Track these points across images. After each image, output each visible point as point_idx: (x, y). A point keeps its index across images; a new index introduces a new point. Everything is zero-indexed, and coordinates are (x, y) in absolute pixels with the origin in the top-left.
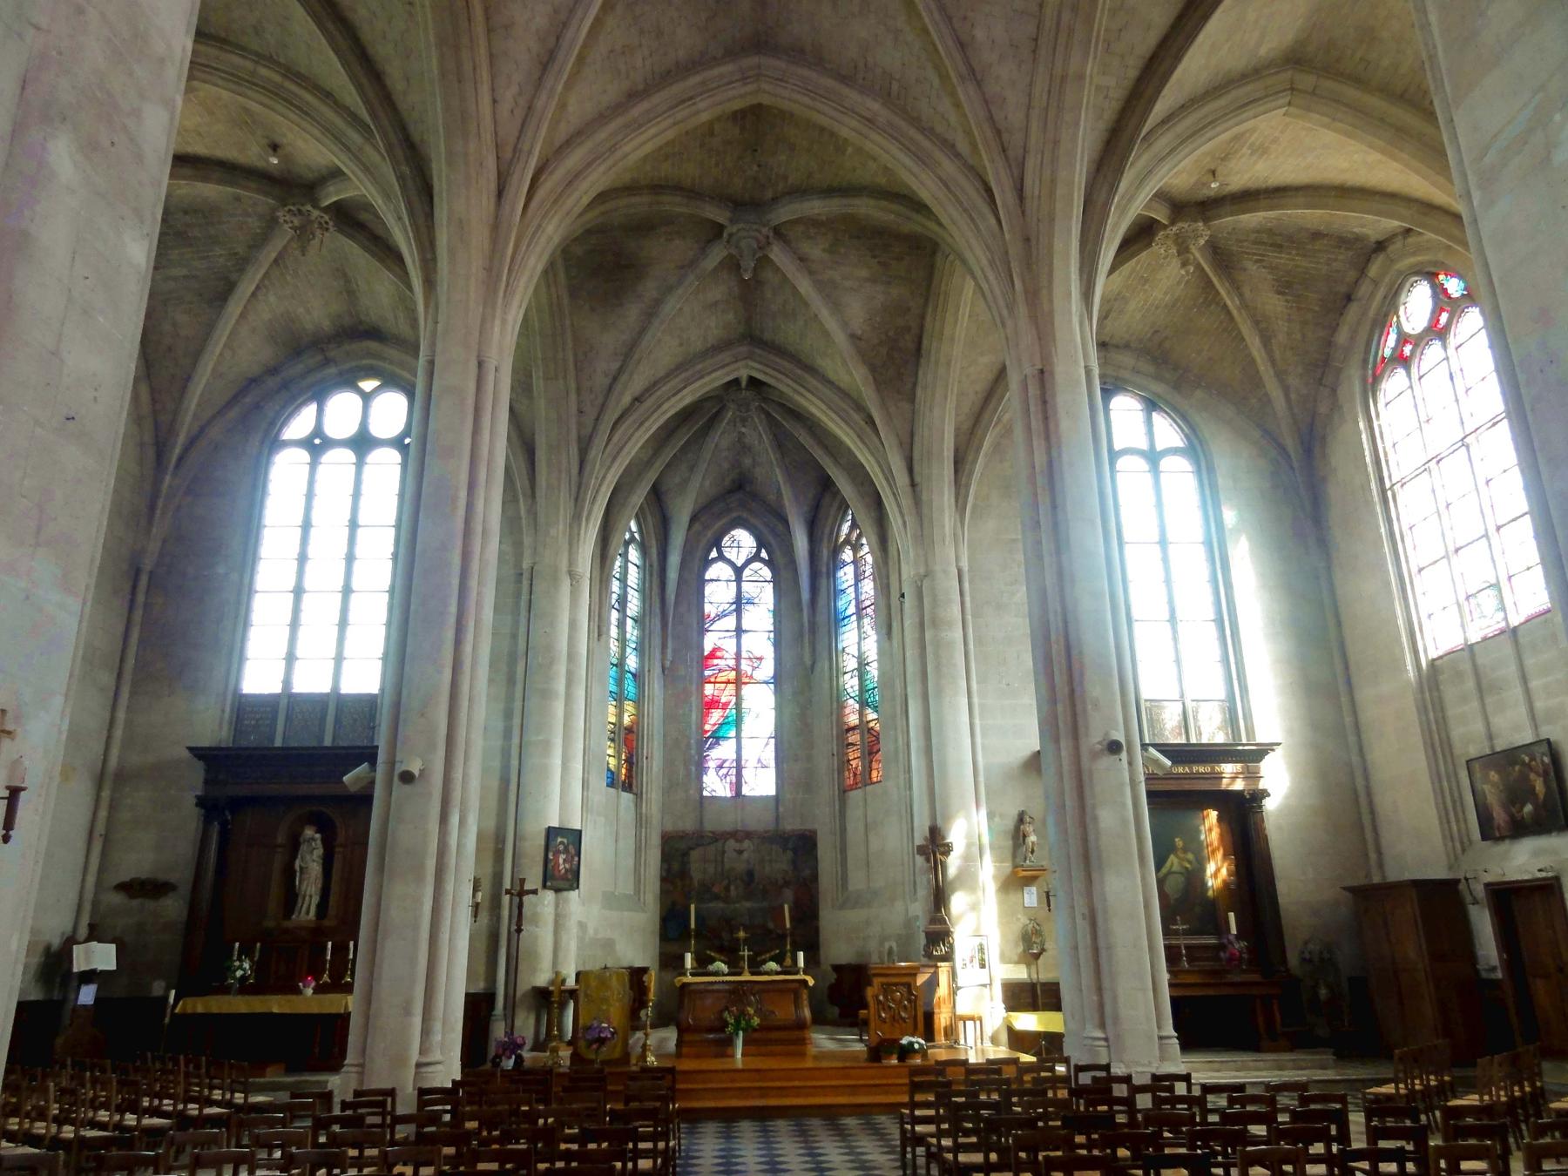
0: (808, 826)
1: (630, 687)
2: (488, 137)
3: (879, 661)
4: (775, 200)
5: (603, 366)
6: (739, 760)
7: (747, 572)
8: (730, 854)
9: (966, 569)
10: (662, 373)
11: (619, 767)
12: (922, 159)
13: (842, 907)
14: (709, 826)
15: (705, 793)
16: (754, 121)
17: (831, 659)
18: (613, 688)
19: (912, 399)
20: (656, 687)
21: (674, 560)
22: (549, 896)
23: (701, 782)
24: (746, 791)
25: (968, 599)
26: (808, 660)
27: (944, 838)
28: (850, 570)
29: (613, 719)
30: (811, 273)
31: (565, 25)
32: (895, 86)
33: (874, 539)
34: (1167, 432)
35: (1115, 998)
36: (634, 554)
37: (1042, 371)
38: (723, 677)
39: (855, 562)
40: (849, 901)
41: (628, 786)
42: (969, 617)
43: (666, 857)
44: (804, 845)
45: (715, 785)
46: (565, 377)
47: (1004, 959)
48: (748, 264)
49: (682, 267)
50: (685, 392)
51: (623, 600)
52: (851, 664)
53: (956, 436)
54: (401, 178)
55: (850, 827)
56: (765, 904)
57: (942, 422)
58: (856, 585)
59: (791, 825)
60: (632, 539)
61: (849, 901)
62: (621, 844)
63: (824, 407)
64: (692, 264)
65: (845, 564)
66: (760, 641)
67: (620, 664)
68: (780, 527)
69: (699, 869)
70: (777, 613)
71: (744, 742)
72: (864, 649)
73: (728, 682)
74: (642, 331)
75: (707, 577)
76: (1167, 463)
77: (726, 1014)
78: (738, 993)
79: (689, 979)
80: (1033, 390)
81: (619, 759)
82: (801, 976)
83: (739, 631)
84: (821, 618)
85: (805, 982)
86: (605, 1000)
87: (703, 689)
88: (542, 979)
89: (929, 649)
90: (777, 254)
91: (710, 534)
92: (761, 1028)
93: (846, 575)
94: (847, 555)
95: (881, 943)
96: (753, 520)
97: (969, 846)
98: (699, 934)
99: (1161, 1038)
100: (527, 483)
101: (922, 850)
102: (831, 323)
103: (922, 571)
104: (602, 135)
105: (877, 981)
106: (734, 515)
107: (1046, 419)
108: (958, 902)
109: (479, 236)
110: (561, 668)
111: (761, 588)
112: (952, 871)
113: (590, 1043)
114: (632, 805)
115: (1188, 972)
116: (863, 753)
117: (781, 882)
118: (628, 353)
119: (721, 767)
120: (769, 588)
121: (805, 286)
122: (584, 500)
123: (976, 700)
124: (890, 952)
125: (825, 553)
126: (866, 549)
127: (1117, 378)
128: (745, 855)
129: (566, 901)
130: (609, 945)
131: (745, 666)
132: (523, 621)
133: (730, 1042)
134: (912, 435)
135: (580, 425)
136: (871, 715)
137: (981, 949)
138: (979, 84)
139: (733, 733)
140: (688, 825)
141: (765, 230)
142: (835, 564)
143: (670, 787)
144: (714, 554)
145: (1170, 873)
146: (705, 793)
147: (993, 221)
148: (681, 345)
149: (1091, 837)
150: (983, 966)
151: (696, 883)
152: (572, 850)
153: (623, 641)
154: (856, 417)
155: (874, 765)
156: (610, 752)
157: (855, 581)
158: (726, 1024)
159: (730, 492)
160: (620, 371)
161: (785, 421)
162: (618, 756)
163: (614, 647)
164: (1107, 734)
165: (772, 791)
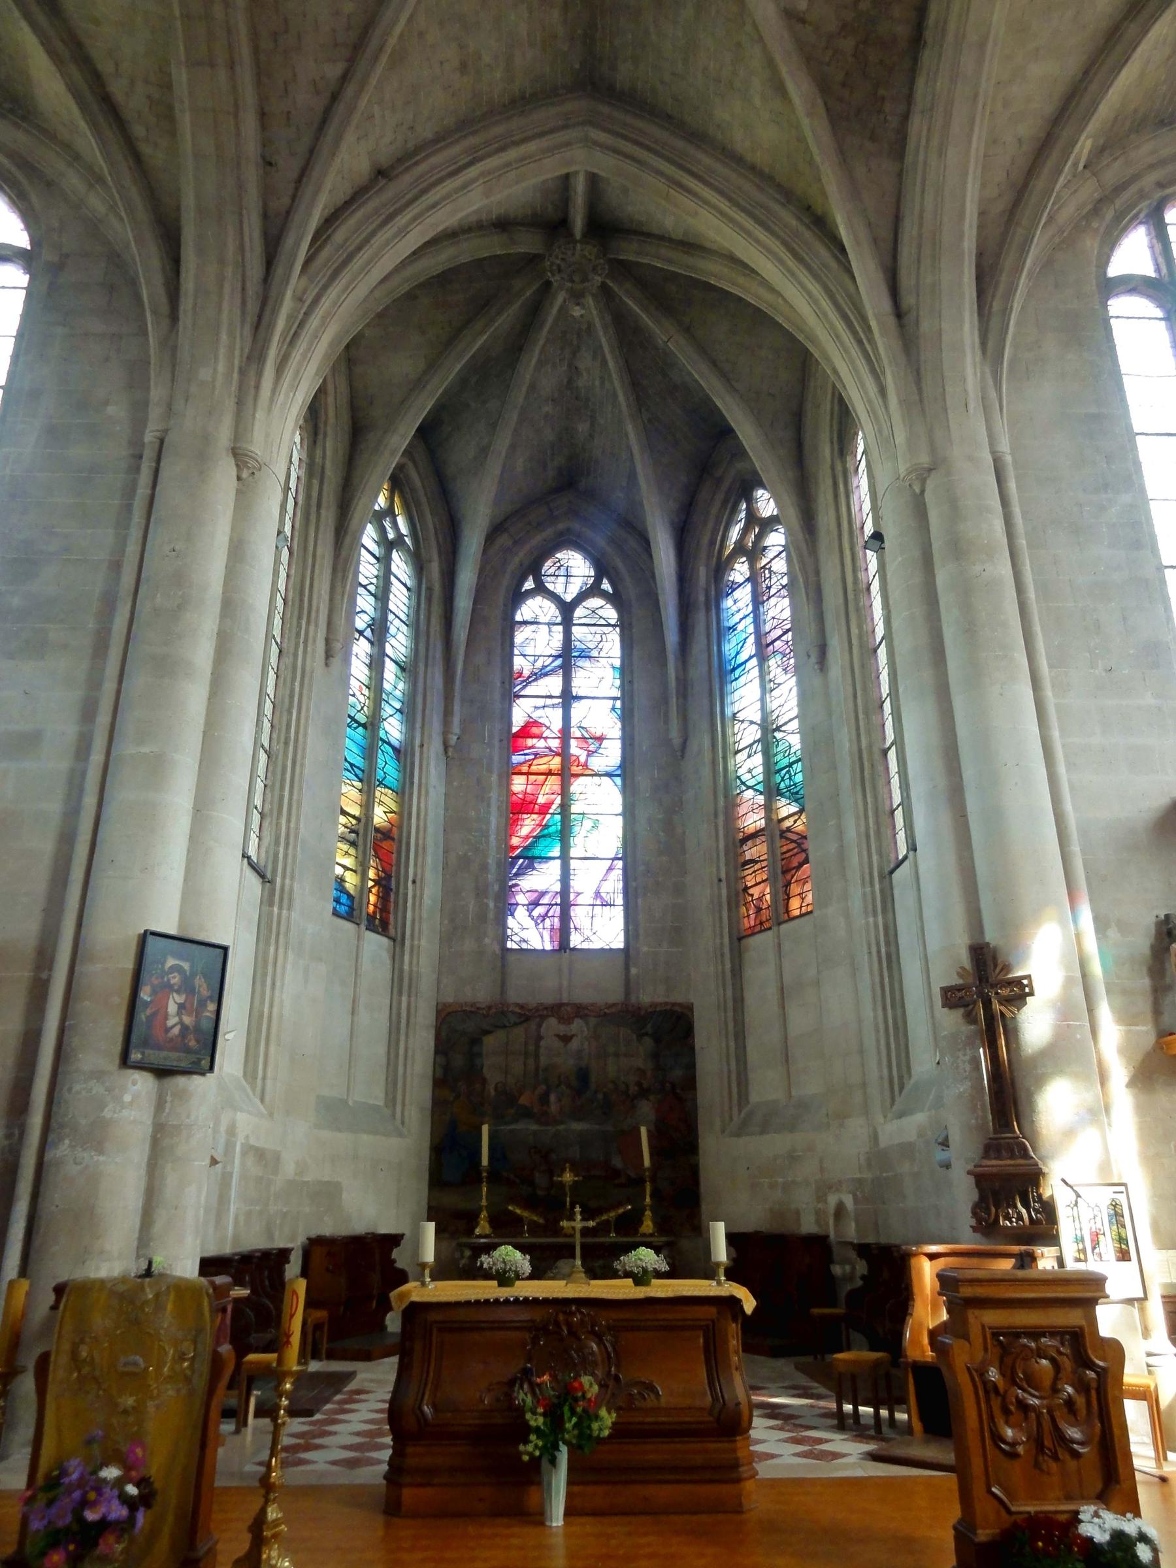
0: (678, 997)
1: (387, 766)
5: (314, 68)
6: (565, 891)
7: (579, 612)
8: (549, 1042)
9: (1008, 459)
10: (427, 132)
11: (363, 890)
14: (515, 996)
18: (358, 761)
19: (898, 148)
20: (432, 772)
21: (467, 578)
22: (141, 1084)
23: (505, 927)
24: (575, 941)
25: (1017, 510)
26: (675, 735)
27: (1007, 968)
28: (744, 595)
29: (355, 811)
36: (400, 566)
38: (540, 765)
39: (753, 579)
40: (750, 1120)
41: (381, 923)
42: (1022, 542)
43: (443, 1047)
44: (672, 1029)
45: (527, 931)
46: (231, 65)
50: (472, 172)
51: (379, 630)
52: (748, 734)
53: (981, 227)
55: (750, 997)
57: (960, 176)
58: (756, 612)
59: (649, 996)
61: (750, 1120)
62: (364, 1017)
63: (724, 205)
65: (734, 587)
66: (599, 714)
67: (372, 725)
68: (633, 543)
69: (498, 1063)
70: (626, 671)
72: (772, 705)
73: (550, 773)
75: (518, 618)
77: (523, 1397)
78: (555, 1330)
81: (364, 877)
83: (568, 698)
84: (697, 672)
86: (136, 1379)
87: (509, 783)
94: (740, 571)
95: (821, 1198)
96: (588, 533)
98: (495, 1176)
100: (161, 292)
103: (924, 459)
106: (561, 526)
108: (1056, 1105)
111: (602, 634)
113: (55, 1538)
114: (386, 957)
117: (633, 1089)
120: (614, 636)
122: (271, 326)
123: (1048, 693)
124: (840, 1211)
125: (702, 574)
128: (574, 1044)
129: (182, 1096)
130: (327, 1193)
131: (574, 749)
132: (135, 533)
133: (532, 1475)
134: (897, 221)
135: (267, 192)
136: (785, 808)
139: (556, 851)
140: (481, 993)
142: (720, 588)
143: (455, 927)
144: (529, 584)
146: (509, 945)
148: (463, 67)
150: (1124, 1256)
152: (202, 986)
155: (795, 889)
156: (349, 862)
157: (757, 605)
160: (345, 78)
162: (361, 870)
165: (617, 941)
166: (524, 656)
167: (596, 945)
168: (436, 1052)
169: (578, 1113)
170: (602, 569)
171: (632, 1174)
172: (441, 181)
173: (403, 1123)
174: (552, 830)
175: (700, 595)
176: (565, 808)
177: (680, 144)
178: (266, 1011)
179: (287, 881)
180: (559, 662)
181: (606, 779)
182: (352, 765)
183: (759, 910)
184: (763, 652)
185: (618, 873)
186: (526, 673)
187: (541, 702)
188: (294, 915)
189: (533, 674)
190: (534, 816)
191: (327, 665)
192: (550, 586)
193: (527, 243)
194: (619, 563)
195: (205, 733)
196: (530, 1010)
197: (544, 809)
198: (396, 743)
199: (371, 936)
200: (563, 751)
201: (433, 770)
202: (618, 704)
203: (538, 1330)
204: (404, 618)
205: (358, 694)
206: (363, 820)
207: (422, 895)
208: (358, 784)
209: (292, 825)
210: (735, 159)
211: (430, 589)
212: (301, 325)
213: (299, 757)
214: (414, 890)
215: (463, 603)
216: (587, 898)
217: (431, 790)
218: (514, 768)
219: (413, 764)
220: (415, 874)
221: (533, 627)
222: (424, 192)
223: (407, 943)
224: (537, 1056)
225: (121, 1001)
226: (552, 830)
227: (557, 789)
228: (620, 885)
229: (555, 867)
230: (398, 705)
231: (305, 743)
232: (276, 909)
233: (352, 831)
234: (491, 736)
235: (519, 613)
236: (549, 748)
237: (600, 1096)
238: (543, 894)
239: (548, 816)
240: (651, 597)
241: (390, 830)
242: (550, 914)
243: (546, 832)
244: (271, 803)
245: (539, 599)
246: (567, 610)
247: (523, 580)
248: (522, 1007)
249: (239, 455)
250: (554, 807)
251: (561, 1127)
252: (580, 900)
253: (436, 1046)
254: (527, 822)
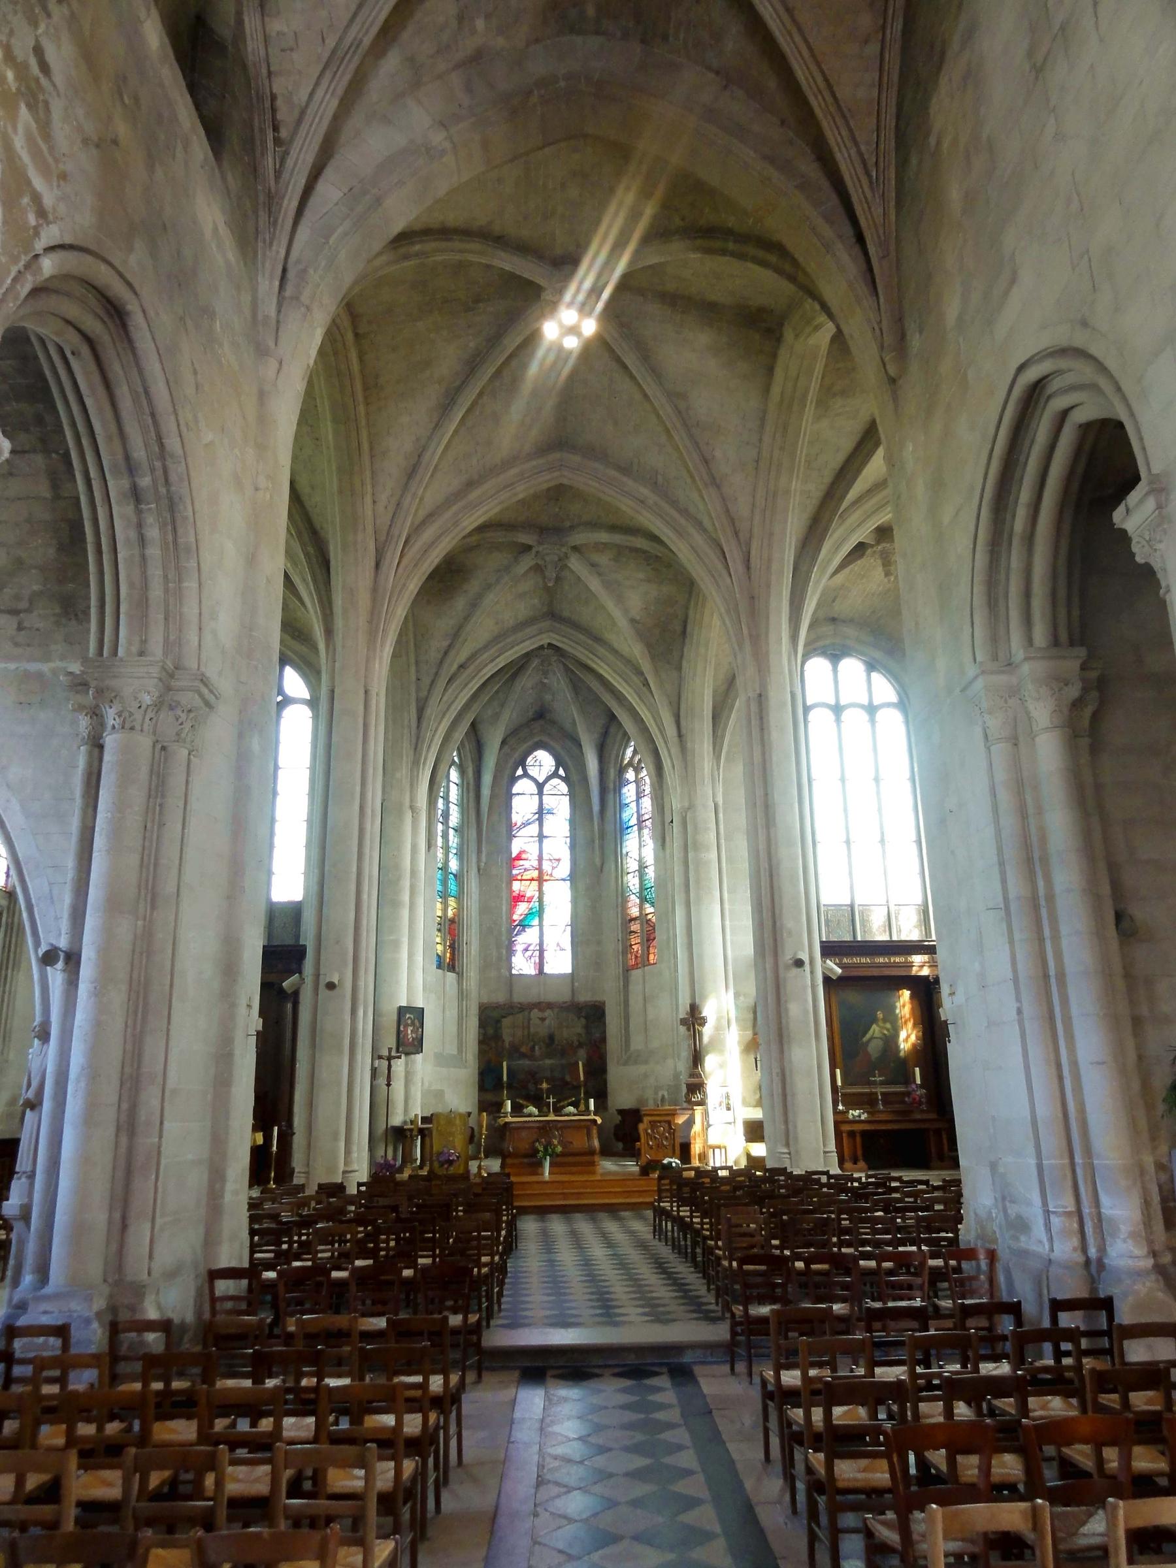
0: (598, 998)
1: (453, 886)
2: (370, 529)
3: (655, 865)
4: (572, 528)
5: (437, 644)
6: (541, 944)
9: (720, 803)
11: (445, 952)
12: (681, 534)
13: (625, 1063)
15: (514, 972)
16: (558, 493)
17: (617, 861)
18: (440, 888)
19: (679, 668)
20: (473, 884)
21: (487, 779)
24: (548, 969)
25: (722, 827)
26: (598, 861)
27: (700, 1013)
29: (439, 913)
30: (600, 574)
31: (425, 449)
32: (660, 479)
33: (651, 767)
34: (884, 689)
35: (795, 1127)
36: (454, 775)
37: (760, 695)
38: (527, 875)
39: (637, 781)
40: (631, 1058)
41: (452, 967)
42: (722, 841)
43: (483, 1024)
44: (594, 1014)
45: (522, 965)
47: (745, 1103)
48: (551, 573)
49: (499, 571)
51: (446, 815)
53: (714, 697)
54: (307, 554)
55: (631, 1002)
56: (564, 1062)
58: (637, 801)
59: (584, 997)
60: (453, 763)
61: (631, 1058)
64: (507, 569)
67: (445, 868)
69: (509, 1032)
70: (572, 822)
72: (643, 855)
73: (532, 880)
74: (467, 618)
75: (514, 791)
76: (881, 715)
78: (545, 1129)
79: (509, 1119)
80: (754, 708)
81: (445, 946)
82: (592, 1117)
83: (541, 837)
84: (609, 827)
85: (595, 1121)
88: (397, 1120)
89: (691, 867)
90: (575, 564)
92: (563, 1154)
93: (629, 792)
94: (630, 775)
95: (656, 1093)
96: (552, 743)
97: (719, 1019)
98: (510, 1086)
99: (825, 1152)
101: (684, 1022)
102: (617, 613)
103: (686, 804)
104: (448, 514)
105: (646, 1119)
107: (762, 729)
108: (710, 1062)
109: (364, 599)
110: (406, 883)
112: (706, 1039)
114: (455, 982)
115: (882, 1112)
116: (642, 939)
117: (576, 1043)
118: (456, 635)
119: (526, 950)
121: (595, 584)
122: (422, 749)
123: (727, 906)
124: (663, 1097)
125: (612, 773)
126: (644, 773)
127: (844, 646)
128: (547, 1022)
129: (414, 1062)
130: (439, 1094)
131: (546, 866)
133: (540, 1164)
135: (418, 690)
136: (649, 909)
137: (728, 1097)
138: (718, 487)
139: (536, 922)
140: (500, 997)
141: (564, 550)
142: (621, 782)
143: (486, 965)
144: (520, 772)
145: (872, 1038)
146: (514, 972)
147: (728, 580)
149: (784, 1021)
150: (728, 1109)
151: (507, 1045)
153: (446, 849)
154: (635, 678)
156: (438, 940)
157: (635, 797)
158: (538, 1151)
159: (533, 720)
160: (450, 646)
161: (580, 677)
163: (440, 854)
164: (795, 954)
169: (549, 1056)
172: (486, 665)
175: (610, 787)
177: (590, 642)
183: (636, 957)
184: (640, 823)
194: (570, 763)
199: (449, 974)
202: (568, 840)
203: (543, 1128)
210: (615, 652)
211: (468, 784)
215: (486, 792)
222: (480, 671)
224: (529, 1028)
225: (394, 1031)
240: (585, 779)
245: (525, 780)
246: (540, 786)
249: (411, 807)
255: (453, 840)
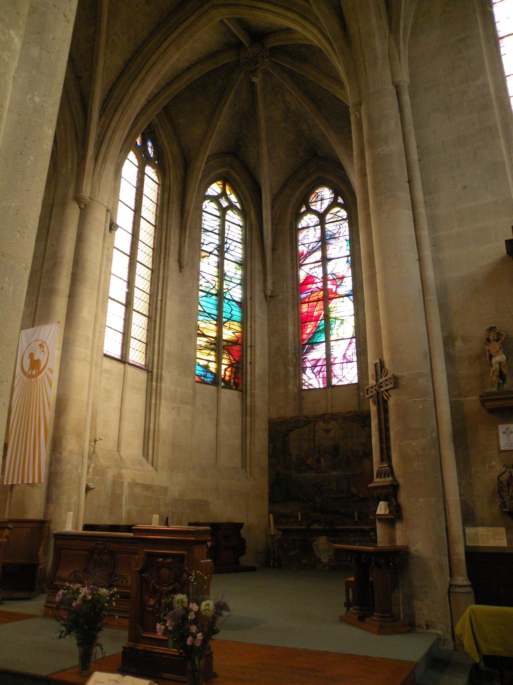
7: (328, 216)
18: (215, 312)
23: (300, 379)
36: (232, 216)
43: (272, 439)
45: (312, 380)
60: (231, 206)
62: (224, 427)
66: (340, 267)
67: (220, 295)
71: (332, 344)
91: (297, 194)
123: (422, 210)
128: (332, 433)
139: (323, 338)
140: (289, 411)
144: (303, 209)
146: (304, 388)
166: (304, 244)
167: (345, 382)
168: (269, 442)
170: (337, 193)
171: (362, 496)
173: (251, 475)
174: (321, 328)
176: (327, 317)
178: (152, 427)
179: (160, 371)
180: (320, 244)
181: (346, 298)
182: (209, 314)
185: (354, 345)
186: (305, 253)
187: (312, 266)
188: (163, 385)
189: (308, 252)
190: (312, 323)
191: (181, 272)
192: (313, 208)
193: (227, 58)
195: (67, 315)
196: (310, 418)
197: (317, 319)
198: (238, 300)
200: (324, 289)
201: (257, 309)
204: (240, 241)
205: (211, 281)
206: (218, 338)
207: (254, 368)
208: (215, 322)
209: (161, 346)
211: (251, 224)
212: (104, 135)
213: (163, 316)
214: (251, 367)
216: (339, 360)
217: (257, 319)
218: (302, 301)
219: (247, 308)
220: (251, 359)
221: (307, 230)
223: (249, 392)
226: (321, 328)
227: (322, 307)
228: (355, 351)
229: (323, 346)
230: (238, 282)
231: (165, 309)
232: (154, 384)
233: (211, 344)
234: (287, 287)
235: (300, 224)
236: (318, 288)
237: (345, 458)
238: (318, 360)
239: (319, 322)
241: (238, 340)
242: (322, 370)
243: (318, 329)
244: (150, 338)
245: (309, 215)
246: (322, 216)
247: (300, 207)
248: (306, 417)
250: (322, 316)
251: (326, 474)
252: (336, 361)
253: (269, 439)
254: (309, 326)
255: (233, 270)
